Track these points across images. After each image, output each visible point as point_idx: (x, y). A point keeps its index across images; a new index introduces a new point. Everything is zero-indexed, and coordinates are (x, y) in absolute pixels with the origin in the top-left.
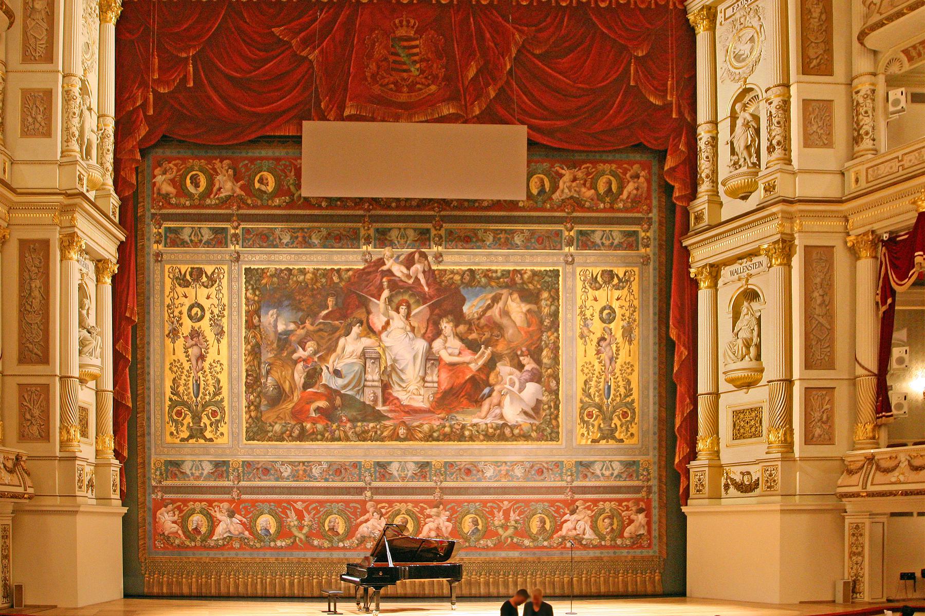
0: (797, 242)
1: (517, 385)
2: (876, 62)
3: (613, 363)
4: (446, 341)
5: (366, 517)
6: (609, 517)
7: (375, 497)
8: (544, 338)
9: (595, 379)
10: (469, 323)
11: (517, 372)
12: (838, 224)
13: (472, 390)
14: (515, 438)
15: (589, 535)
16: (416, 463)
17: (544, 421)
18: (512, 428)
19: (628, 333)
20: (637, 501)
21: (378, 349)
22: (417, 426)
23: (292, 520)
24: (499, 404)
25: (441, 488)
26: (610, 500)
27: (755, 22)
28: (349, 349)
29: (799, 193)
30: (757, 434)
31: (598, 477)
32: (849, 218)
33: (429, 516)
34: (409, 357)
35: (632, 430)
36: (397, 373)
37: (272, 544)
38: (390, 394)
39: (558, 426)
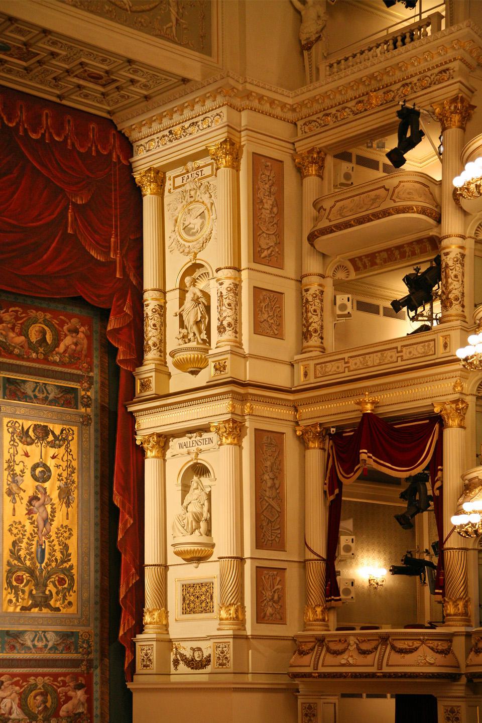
0: (247, 424)
2: (324, 265)
3: (48, 526)
6: (41, 694)
9: (25, 540)
12: (287, 413)
19: (65, 494)
20: (76, 676)
27: (205, 198)
29: (248, 377)
30: (208, 609)
31: (29, 648)
32: (299, 408)
35: (69, 599)
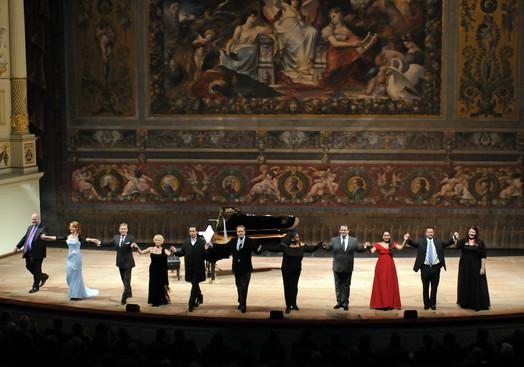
1: (401, 67)
3: (493, 48)
4: (334, 29)
5: (259, 178)
7: (268, 161)
8: (427, 25)
10: (356, 13)
11: (401, 55)
13: (360, 70)
14: (398, 112)
15: (466, 195)
16: (306, 132)
17: (426, 97)
18: (396, 103)
21: (271, 35)
22: (308, 101)
23: (193, 179)
24: (384, 83)
25: (328, 154)
26: (487, 167)
28: (244, 35)
33: (317, 177)
34: (299, 42)
36: (289, 57)
37: (175, 200)
38: (282, 74)
39: (439, 102)
